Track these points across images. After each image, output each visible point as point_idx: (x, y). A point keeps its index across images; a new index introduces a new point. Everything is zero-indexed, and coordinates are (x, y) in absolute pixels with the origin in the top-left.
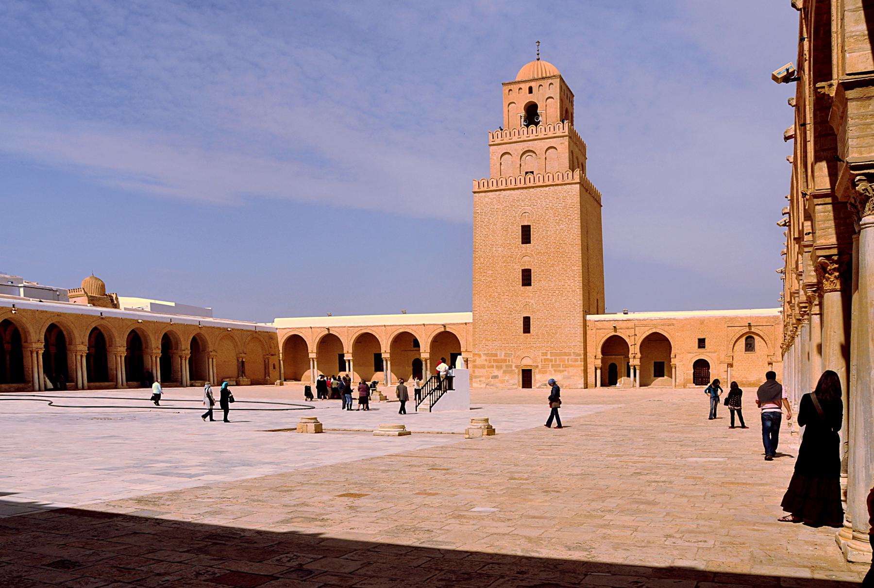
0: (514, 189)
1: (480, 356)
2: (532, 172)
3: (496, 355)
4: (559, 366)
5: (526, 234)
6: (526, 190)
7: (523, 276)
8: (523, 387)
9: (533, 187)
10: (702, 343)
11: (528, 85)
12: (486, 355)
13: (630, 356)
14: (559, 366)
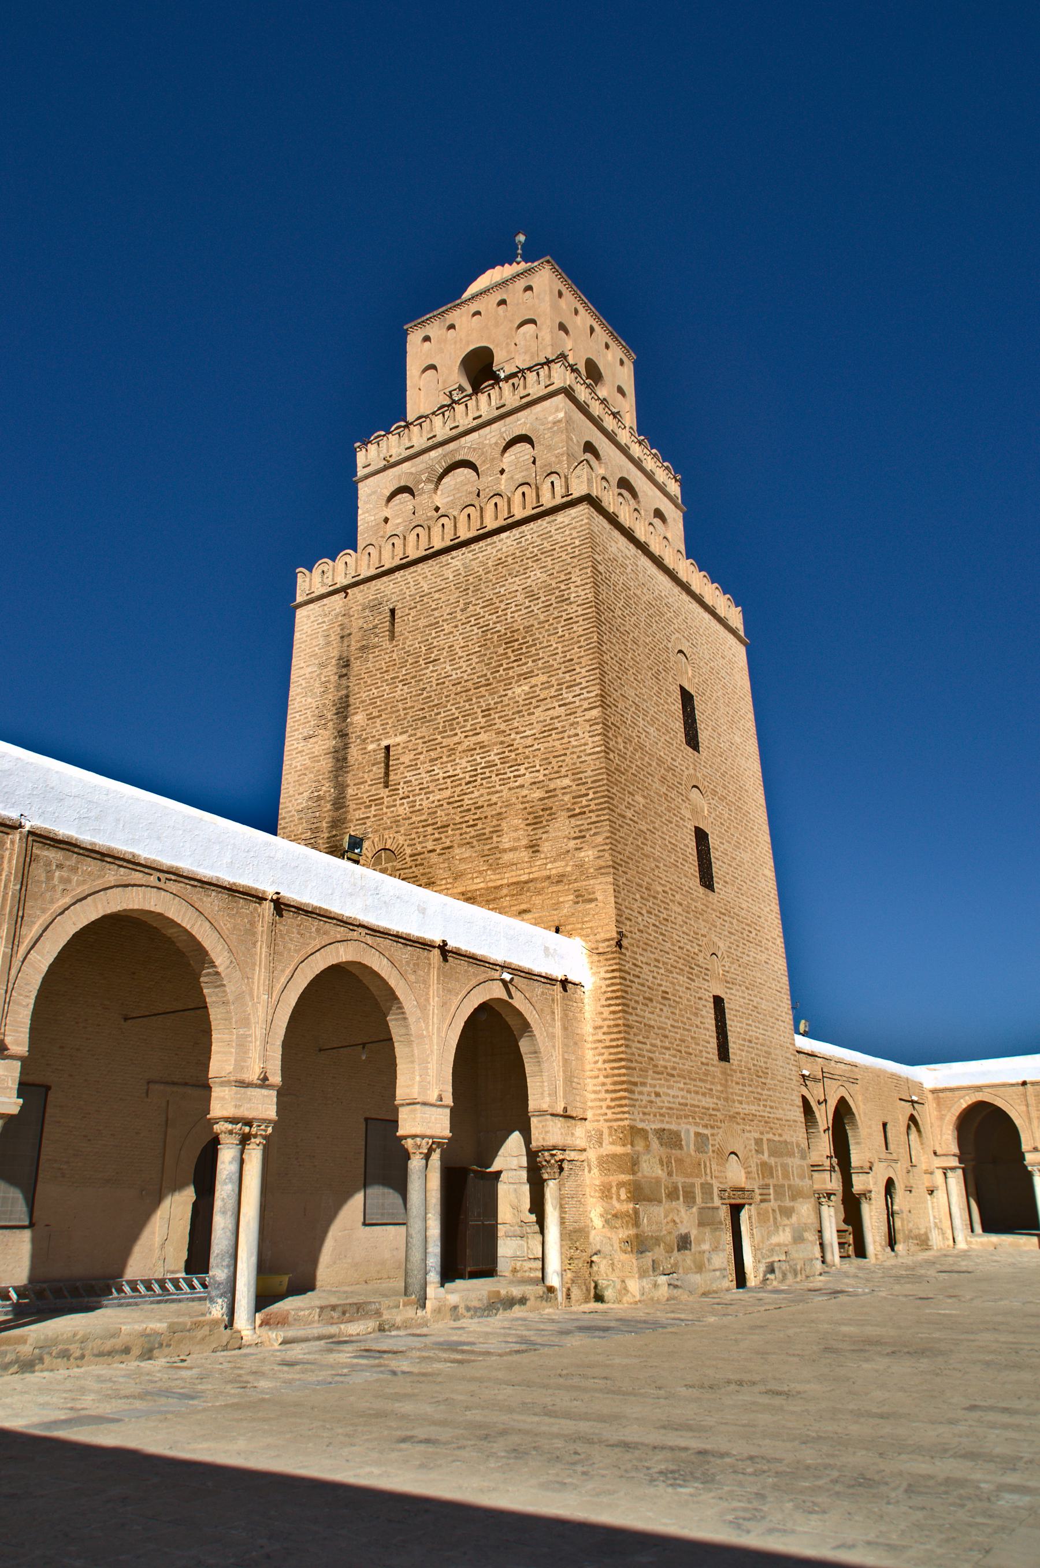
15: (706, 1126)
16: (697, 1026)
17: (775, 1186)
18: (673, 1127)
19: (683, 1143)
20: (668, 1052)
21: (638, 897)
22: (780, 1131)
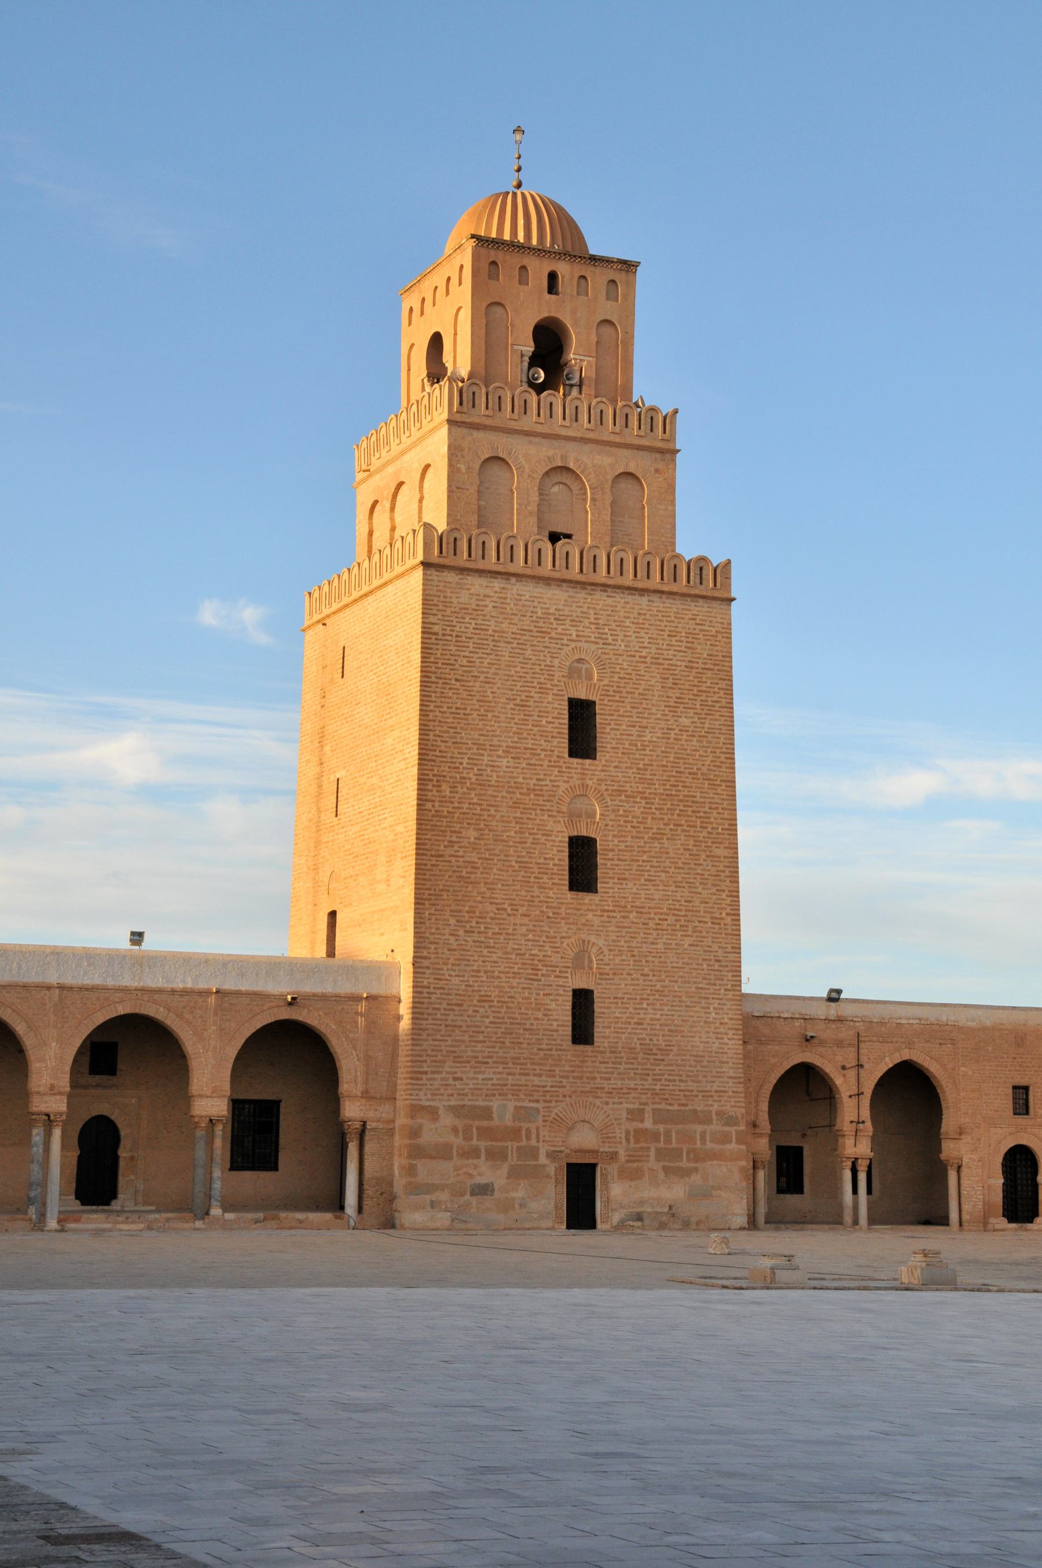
0: (547, 581)
1: (433, 1113)
2: (569, 536)
3: (486, 1113)
4: (677, 1154)
5: (582, 728)
6: (581, 595)
7: (571, 857)
8: (569, 1227)
9: (605, 586)
10: (1022, 1099)
11: (548, 266)
12: (457, 1111)
13: (847, 1128)
14: (677, 1154)
15: (538, 1101)
16: (536, 1019)
17: (658, 1151)
18: (481, 1104)
19: (495, 1115)
20: (480, 1045)
21: (452, 921)
22: (684, 1102)
